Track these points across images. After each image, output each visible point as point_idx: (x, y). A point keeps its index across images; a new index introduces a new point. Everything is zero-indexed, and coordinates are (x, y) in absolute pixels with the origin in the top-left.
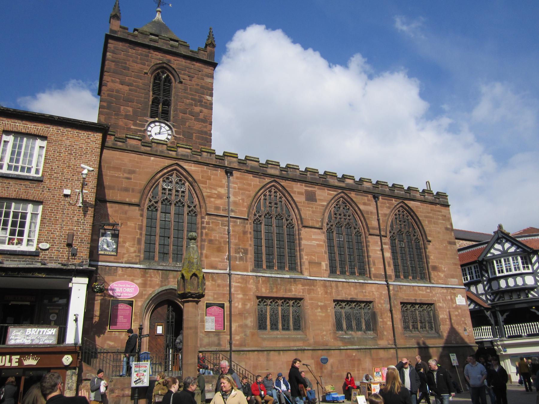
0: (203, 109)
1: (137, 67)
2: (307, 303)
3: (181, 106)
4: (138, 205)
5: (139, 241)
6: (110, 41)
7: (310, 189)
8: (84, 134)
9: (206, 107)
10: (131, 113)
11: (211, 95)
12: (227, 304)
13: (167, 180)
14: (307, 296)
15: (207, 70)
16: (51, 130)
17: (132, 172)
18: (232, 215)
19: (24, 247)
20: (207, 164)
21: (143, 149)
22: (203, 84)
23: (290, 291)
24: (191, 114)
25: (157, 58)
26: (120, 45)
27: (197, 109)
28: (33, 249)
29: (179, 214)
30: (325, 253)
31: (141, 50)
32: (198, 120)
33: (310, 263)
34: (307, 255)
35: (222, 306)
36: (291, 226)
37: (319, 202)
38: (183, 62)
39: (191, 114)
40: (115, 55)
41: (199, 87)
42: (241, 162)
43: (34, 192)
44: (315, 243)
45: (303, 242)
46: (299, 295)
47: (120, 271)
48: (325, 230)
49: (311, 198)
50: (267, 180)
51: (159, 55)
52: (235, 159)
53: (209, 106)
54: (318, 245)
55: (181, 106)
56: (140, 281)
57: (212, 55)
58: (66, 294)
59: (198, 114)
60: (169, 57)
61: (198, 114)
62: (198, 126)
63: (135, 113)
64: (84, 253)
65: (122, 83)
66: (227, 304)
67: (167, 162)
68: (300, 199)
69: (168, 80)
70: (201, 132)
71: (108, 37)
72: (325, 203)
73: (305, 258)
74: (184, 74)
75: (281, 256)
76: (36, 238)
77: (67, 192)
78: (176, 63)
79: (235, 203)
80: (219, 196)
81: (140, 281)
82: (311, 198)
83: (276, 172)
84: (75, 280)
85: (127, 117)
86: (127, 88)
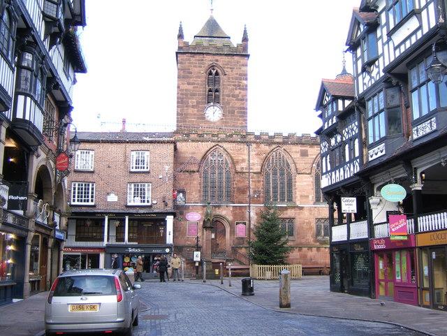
0: (241, 91)
1: (197, 70)
2: (297, 223)
3: (226, 92)
4: (198, 171)
5: (200, 191)
6: (179, 55)
7: (303, 148)
8: (165, 146)
9: (243, 89)
10: (195, 104)
11: (246, 79)
12: (247, 222)
13: (213, 155)
14: (297, 217)
15: (242, 60)
16: (151, 146)
17: (194, 153)
18: (251, 171)
19: (146, 204)
20: (234, 142)
21: (198, 139)
22: (241, 72)
23: (287, 214)
24: (233, 96)
25: (208, 60)
26: (185, 56)
27: (237, 92)
28: (149, 204)
29: (220, 174)
30: (312, 189)
31: (198, 57)
32: (238, 100)
33: (301, 196)
34: (300, 191)
35: (245, 224)
36: (289, 175)
37: (309, 157)
38: (226, 59)
39: (233, 96)
40: (183, 65)
41: (238, 76)
42: (257, 137)
43: (147, 178)
44: (305, 183)
45: (297, 184)
46: (293, 216)
47: (191, 208)
48: (313, 174)
49: (304, 154)
50: (274, 146)
51: (210, 58)
52: (252, 137)
53: (245, 88)
54: (308, 185)
55: (226, 92)
56: (201, 212)
57: (245, 48)
58: (165, 222)
59: (238, 96)
60: (217, 57)
61: (238, 96)
62: (238, 104)
63: (198, 103)
64: (170, 204)
65: (189, 84)
66: (247, 222)
67: (214, 144)
68: (296, 156)
69: (217, 74)
70: (241, 108)
71: (177, 53)
72: (315, 157)
73: (298, 193)
74: (227, 68)
75: (282, 193)
76: (150, 200)
77: (161, 177)
78: (222, 61)
79: (254, 164)
80: (243, 160)
81: (201, 212)
82: (304, 154)
83: (280, 140)
84: (168, 216)
85: (193, 107)
86: (191, 87)
